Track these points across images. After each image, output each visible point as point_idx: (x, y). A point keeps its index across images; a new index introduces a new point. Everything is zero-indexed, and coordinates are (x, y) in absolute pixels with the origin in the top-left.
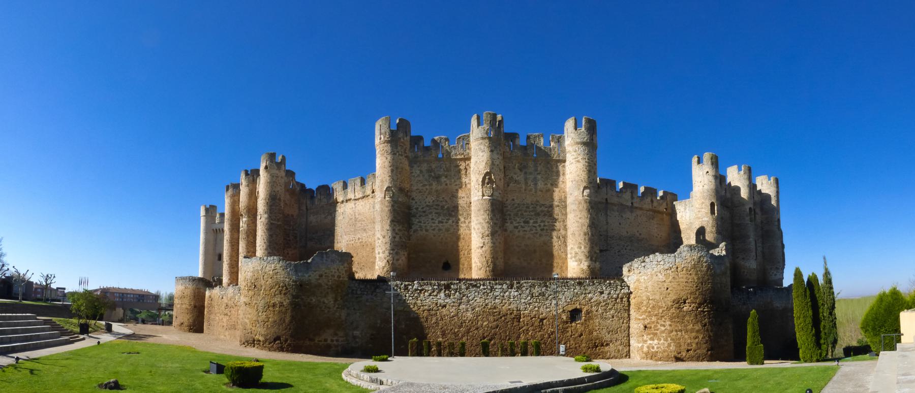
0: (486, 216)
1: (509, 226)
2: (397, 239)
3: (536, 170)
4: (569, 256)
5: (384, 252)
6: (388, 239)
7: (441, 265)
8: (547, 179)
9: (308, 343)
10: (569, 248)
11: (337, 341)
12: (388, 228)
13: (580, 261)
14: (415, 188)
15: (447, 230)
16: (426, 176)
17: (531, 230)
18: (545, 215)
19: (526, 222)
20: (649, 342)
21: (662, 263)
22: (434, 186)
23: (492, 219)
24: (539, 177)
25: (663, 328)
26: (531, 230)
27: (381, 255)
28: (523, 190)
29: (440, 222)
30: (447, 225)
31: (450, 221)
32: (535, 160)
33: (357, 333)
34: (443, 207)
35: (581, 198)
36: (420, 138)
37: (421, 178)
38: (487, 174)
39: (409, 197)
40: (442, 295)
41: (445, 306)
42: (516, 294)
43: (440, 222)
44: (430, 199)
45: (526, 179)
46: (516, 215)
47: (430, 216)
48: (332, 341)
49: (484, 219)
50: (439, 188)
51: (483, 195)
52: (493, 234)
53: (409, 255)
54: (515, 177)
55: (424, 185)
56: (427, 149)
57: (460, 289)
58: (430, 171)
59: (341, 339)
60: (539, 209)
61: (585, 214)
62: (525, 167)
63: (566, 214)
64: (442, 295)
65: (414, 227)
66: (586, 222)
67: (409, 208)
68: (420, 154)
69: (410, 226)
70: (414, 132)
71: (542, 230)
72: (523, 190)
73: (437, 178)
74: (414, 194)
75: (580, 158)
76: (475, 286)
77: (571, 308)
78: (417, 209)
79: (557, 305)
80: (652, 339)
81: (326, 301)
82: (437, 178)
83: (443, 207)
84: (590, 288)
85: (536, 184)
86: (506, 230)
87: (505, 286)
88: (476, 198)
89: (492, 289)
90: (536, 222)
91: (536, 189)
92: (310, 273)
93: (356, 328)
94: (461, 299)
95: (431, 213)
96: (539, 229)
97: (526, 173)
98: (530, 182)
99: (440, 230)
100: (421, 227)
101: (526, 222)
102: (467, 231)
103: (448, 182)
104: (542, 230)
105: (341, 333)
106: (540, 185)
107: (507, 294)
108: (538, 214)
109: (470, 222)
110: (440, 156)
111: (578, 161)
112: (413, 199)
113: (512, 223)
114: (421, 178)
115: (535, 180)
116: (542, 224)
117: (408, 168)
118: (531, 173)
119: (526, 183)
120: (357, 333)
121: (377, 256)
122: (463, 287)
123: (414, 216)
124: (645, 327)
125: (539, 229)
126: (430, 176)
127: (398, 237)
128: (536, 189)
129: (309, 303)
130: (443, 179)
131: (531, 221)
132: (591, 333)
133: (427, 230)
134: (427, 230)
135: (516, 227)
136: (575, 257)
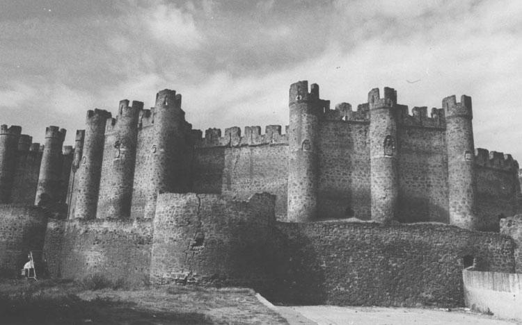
0: (388, 171)
1: (403, 182)
4: (452, 209)
5: (300, 197)
6: (305, 185)
10: (451, 203)
12: (305, 176)
13: (464, 214)
17: (419, 185)
23: (392, 175)
26: (419, 185)
27: (297, 199)
35: (463, 160)
38: (388, 137)
49: (387, 174)
51: (385, 154)
52: (394, 185)
61: (468, 174)
63: (448, 174)
66: (469, 180)
75: (462, 128)
88: (378, 156)
96: (425, 185)
99: (344, 181)
102: (367, 184)
109: (369, 176)
111: (460, 131)
112: (321, 152)
121: (293, 201)
123: (322, 167)
125: (425, 185)
126: (336, 134)
133: (333, 181)
135: (407, 182)
136: (459, 210)
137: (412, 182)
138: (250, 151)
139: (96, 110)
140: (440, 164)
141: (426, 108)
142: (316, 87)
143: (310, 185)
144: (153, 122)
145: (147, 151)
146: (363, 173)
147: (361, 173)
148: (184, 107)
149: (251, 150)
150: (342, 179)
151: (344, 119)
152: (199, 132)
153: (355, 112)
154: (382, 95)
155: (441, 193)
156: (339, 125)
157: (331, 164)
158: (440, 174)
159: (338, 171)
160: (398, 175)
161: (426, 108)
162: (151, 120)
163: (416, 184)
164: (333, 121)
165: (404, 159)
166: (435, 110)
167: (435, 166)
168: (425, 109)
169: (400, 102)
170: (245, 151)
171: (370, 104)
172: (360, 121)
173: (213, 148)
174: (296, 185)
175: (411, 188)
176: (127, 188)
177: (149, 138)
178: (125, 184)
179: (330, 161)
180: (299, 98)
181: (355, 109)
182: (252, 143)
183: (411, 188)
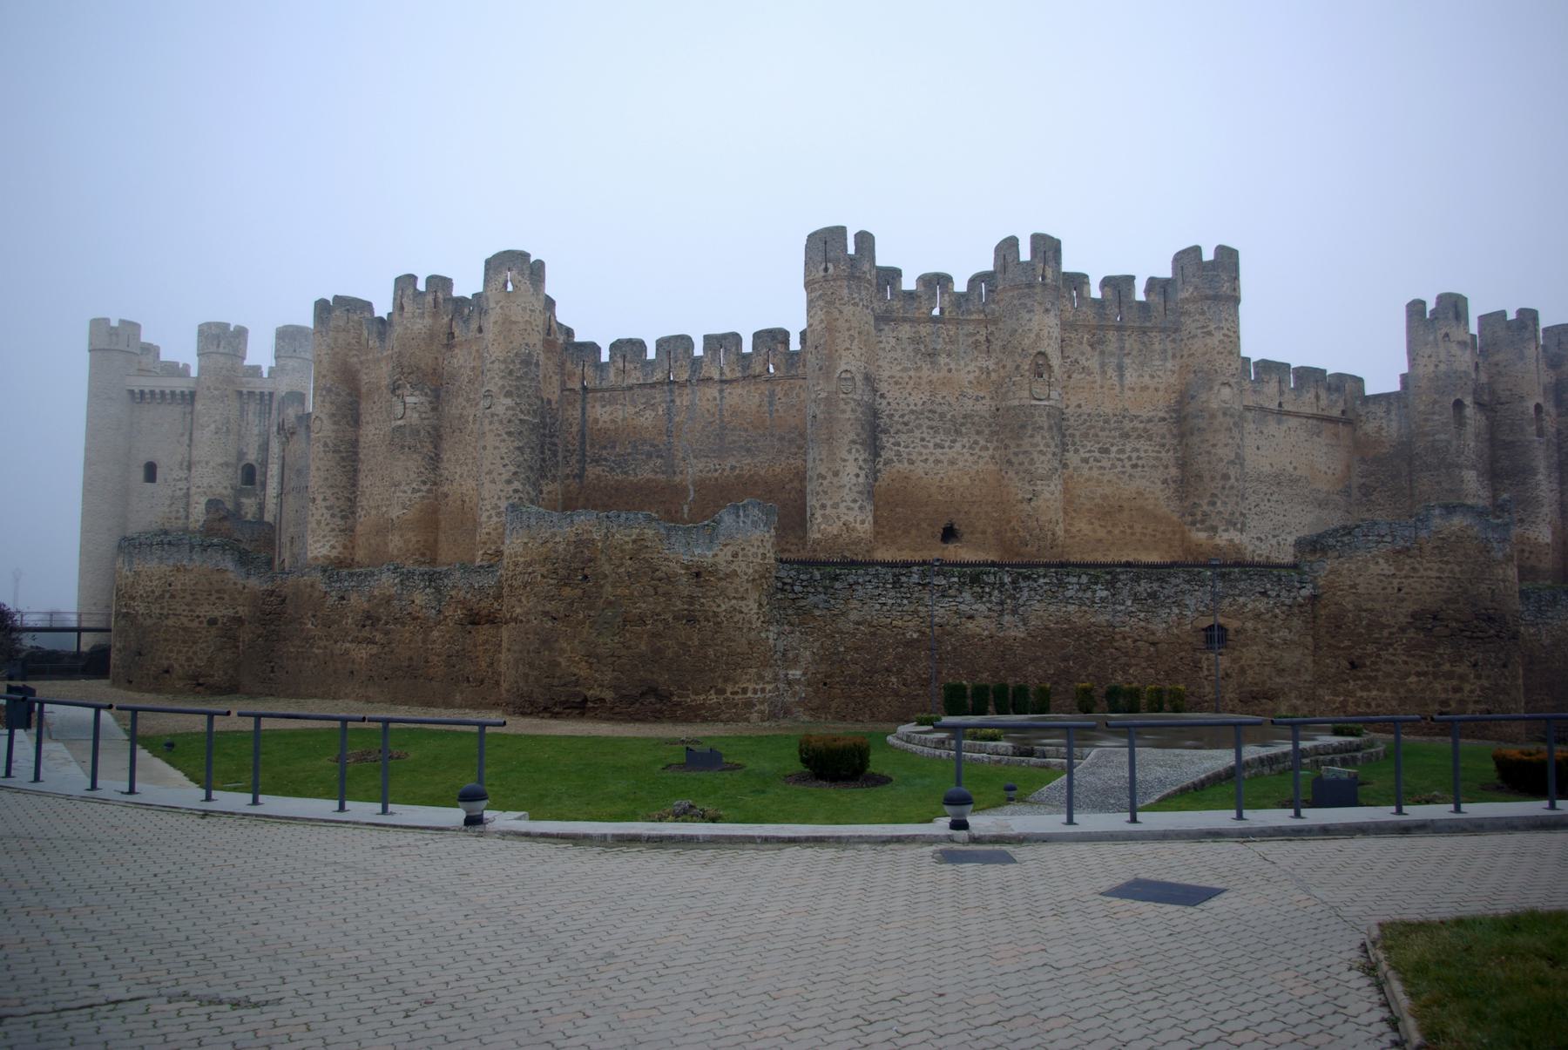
2: (861, 480)
3: (1122, 348)
7: (939, 531)
8: (1142, 364)
9: (713, 698)
11: (763, 690)
14: (886, 374)
15: (952, 462)
16: (910, 349)
17: (1114, 466)
18: (1140, 436)
19: (1107, 451)
20: (1359, 694)
21: (1388, 539)
22: (926, 371)
24: (1127, 361)
25: (1389, 668)
28: (1097, 386)
29: (937, 446)
30: (951, 453)
31: (958, 445)
32: (1119, 328)
33: (796, 673)
34: (942, 416)
36: (894, 274)
37: (899, 354)
39: (875, 391)
40: (967, 596)
41: (971, 617)
42: (1105, 593)
43: (937, 446)
44: (917, 399)
45: (1103, 365)
46: (1085, 435)
47: (917, 433)
48: (755, 692)
50: (935, 376)
53: (876, 510)
54: (1083, 362)
55: (905, 370)
56: (910, 295)
57: (1003, 584)
58: (916, 340)
59: (769, 687)
60: (1127, 425)
62: (1101, 342)
64: (967, 596)
65: (885, 455)
67: (875, 414)
68: (897, 304)
69: (877, 455)
70: (881, 261)
71: (1135, 466)
72: (1097, 386)
73: (932, 355)
74: (883, 387)
76: (1028, 578)
77: (1207, 622)
78: (891, 416)
79: (1181, 616)
80: (1364, 688)
81: (745, 610)
82: (932, 355)
83: (942, 416)
84: (1242, 585)
85: (1121, 376)
86: (1065, 466)
87: (1084, 579)
89: (1062, 585)
90: (1121, 451)
91: (1122, 386)
92: (716, 549)
93: (795, 662)
94: (1002, 603)
95: (919, 427)
96: (1128, 464)
97: (1102, 353)
98: (1110, 372)
99: (937, 462)
100: (898, 454)
101: (1107, 451)
103: (953, 366)
104: (1135, 466)
105: (768, 674)
106: (1131, 377)
107: (1089, 594)
108: (1126, 436)
110: (936, 312)
112: (882, 396)
113: (1076, 451)
114: (899, 354)
115: (1120, 368)
116: (1134, 455)
117: (873, 332)
118: (1112, 354)
119: (1104, 372)
120: (796, 673)
122: (1007, 580)
123: (885, 431)
124: (1353, 665)
125: (1128, 464)
126: (917, 351)
127: (862, 474)
128: (1122, 386)
129: (716, 615)
130: (943, 360)
131: (1114, 449)
132: (1243, 671)
133: (911, 462)
134: (911, 462)
135: (1086, 461)
137: (1096, 460)
138: (717, 395)
139: (336, 298)
140: (1161, 414)
141: (1133, 278)
142: (865, 240)
143: (857, 476)
144: (480, 330)
145: (468, 400)
146: (982, 442)
147: (976, 443)
148: (551, 288)
149: (721, 391)
150: (932, 459)
151: (936, 312)
152: (594, 348)
153: (962, 295)
154: (1025, 254)
155: (1165, 482)
156: (924, 330)
157: (906, 424)
158: (1163, 437)
159: (923, 440)
160: (1064, 444)
161: (1133, 278)
162: (474, 326)
163: (1105, 463)
164: (914, 321)
165: (1079, 406)
166: (1152, 283)
167: (1150, 420)
168: (1130, 279)
169: (1069, 265)
170: (713, 392)
171: (999, 276)
172: (975, 317)
173: (631, 388)
174: (824, 478)
175: (1095, 473)
176: (430, 491)
177: (474, 368)
178: (424, 483)
179: (902, 416)
180: (826, 270)
181: (960, 286)
182: (722, 374)
183: (1095, 473)
